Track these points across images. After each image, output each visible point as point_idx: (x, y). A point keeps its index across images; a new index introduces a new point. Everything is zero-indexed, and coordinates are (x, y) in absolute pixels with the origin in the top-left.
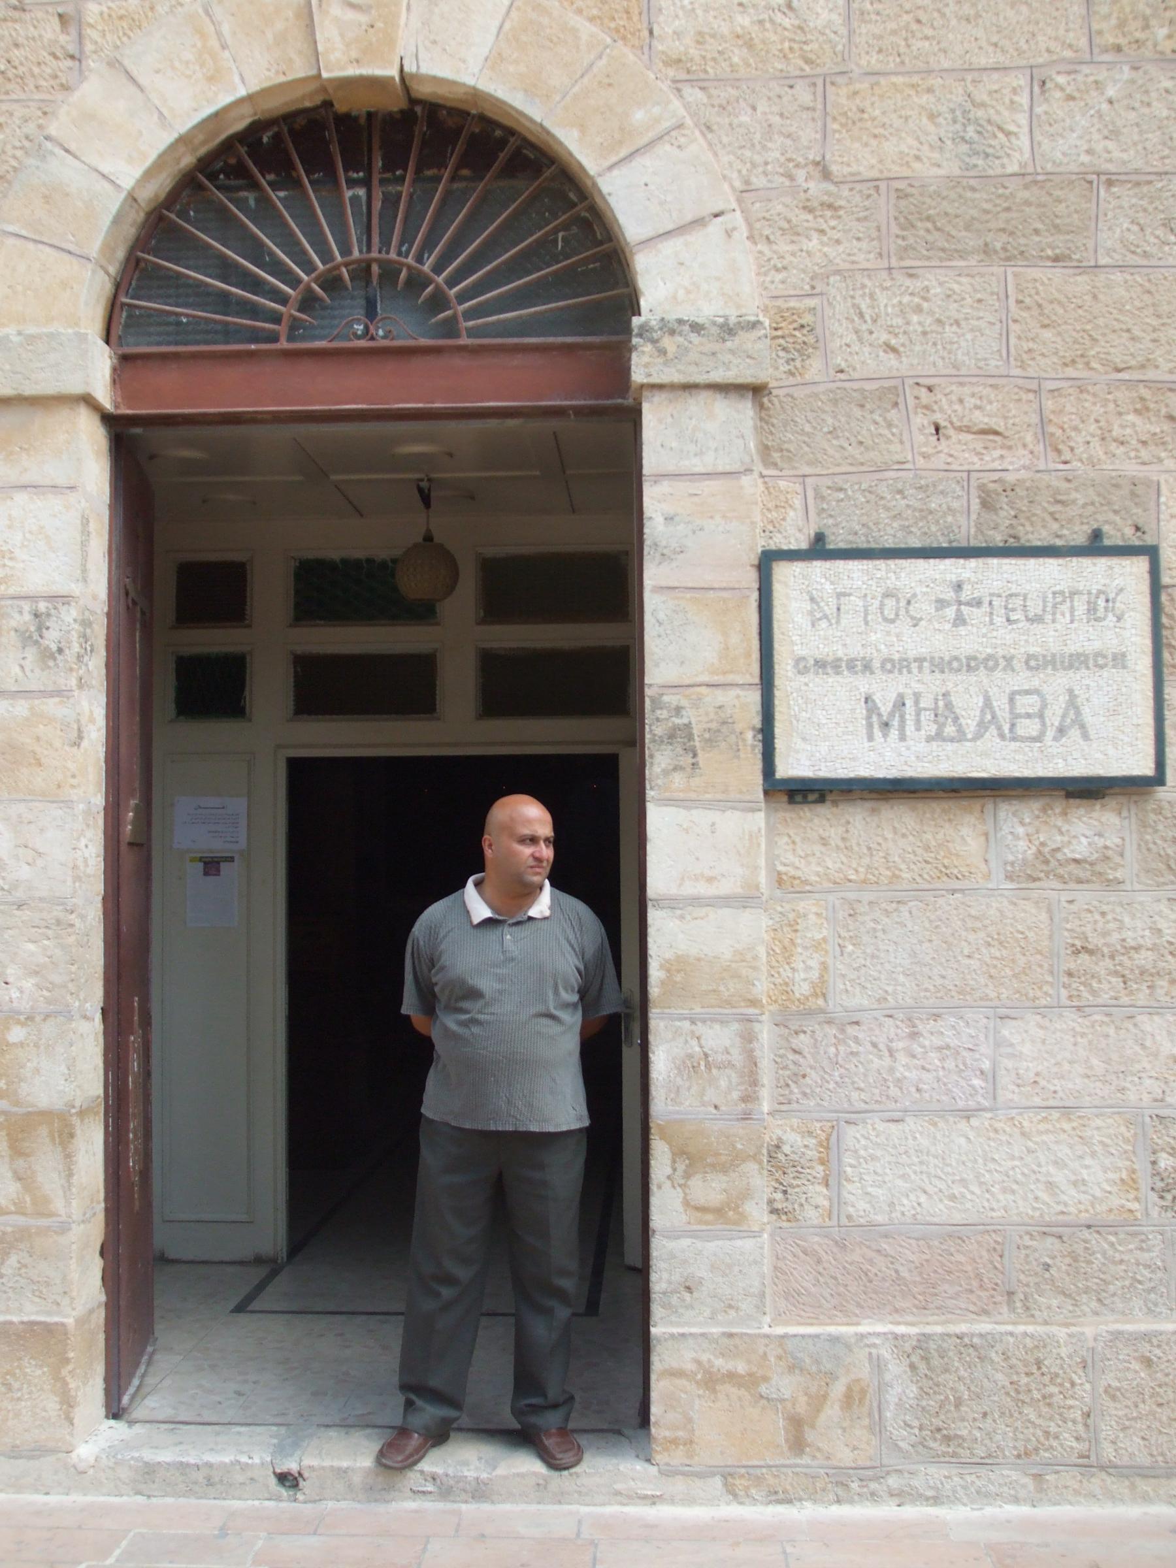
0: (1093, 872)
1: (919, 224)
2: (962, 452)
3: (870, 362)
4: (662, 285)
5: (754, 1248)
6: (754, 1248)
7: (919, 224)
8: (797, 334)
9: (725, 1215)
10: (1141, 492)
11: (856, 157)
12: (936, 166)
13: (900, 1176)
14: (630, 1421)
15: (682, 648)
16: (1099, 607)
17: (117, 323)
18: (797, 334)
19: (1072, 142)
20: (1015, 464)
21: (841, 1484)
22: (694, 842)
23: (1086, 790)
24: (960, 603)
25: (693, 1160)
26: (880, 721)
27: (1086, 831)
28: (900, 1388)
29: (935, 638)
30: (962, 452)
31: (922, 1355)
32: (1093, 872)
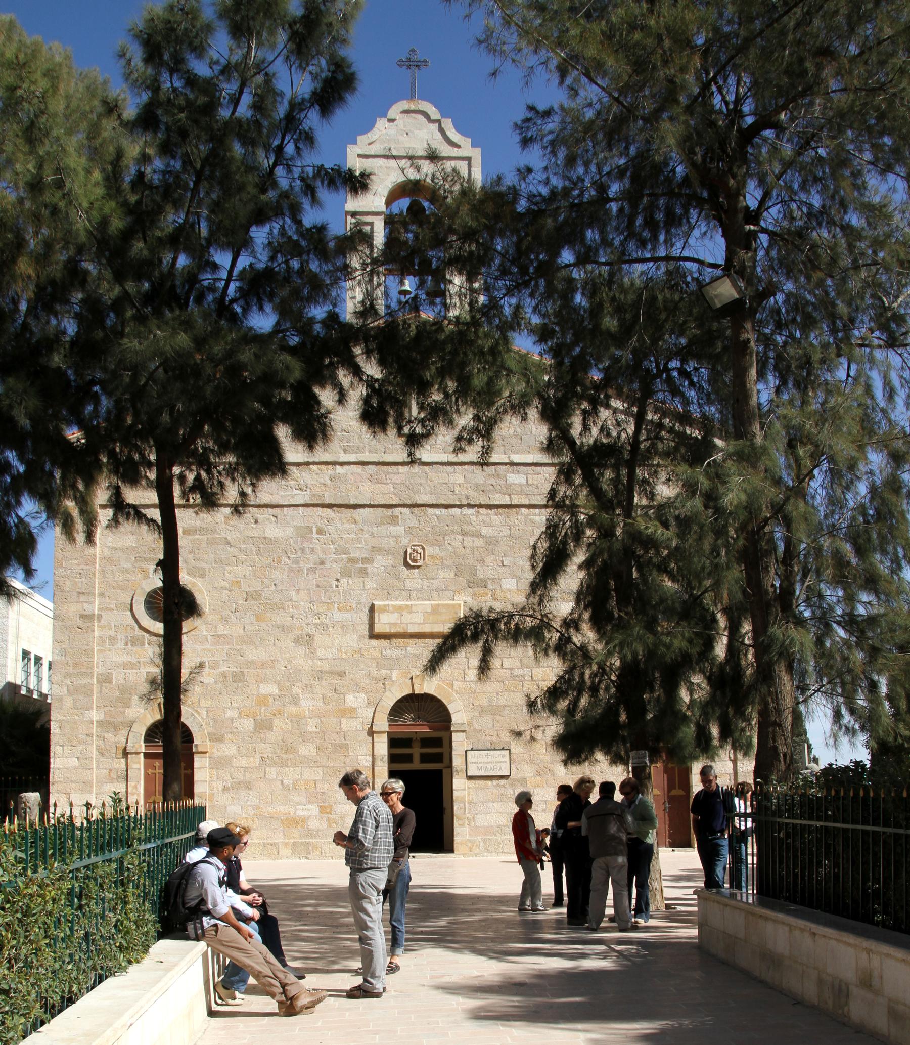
0: (503, 786)
1: (483, 711)
2: (489, 738)
3: (479, 728)
4: (455, 719)
5: (466, 829)
6: (466, 829)
7: (483, 711)
8: (470, 724)
9: (462, 825)
10: (509, 743)
11: (477, 703)
12: (486, 704)
13: (482, 820)
14: (451, 851)
15: (457, 761)
16: (503, 756)
17: (390, 720)
18: (470, 724)
19: (502, 701)
20: (495, 739)
21: (476, 855)
22: (459, 784)
23: (502, 777)
24: (488, 755)
25: (459, 819)
26: (479, 769)
27: (502, 782)
28: (482, 844)
29: (486, 760)
30: (489, 738)
31: (484, 841)
32: (503, 786)
